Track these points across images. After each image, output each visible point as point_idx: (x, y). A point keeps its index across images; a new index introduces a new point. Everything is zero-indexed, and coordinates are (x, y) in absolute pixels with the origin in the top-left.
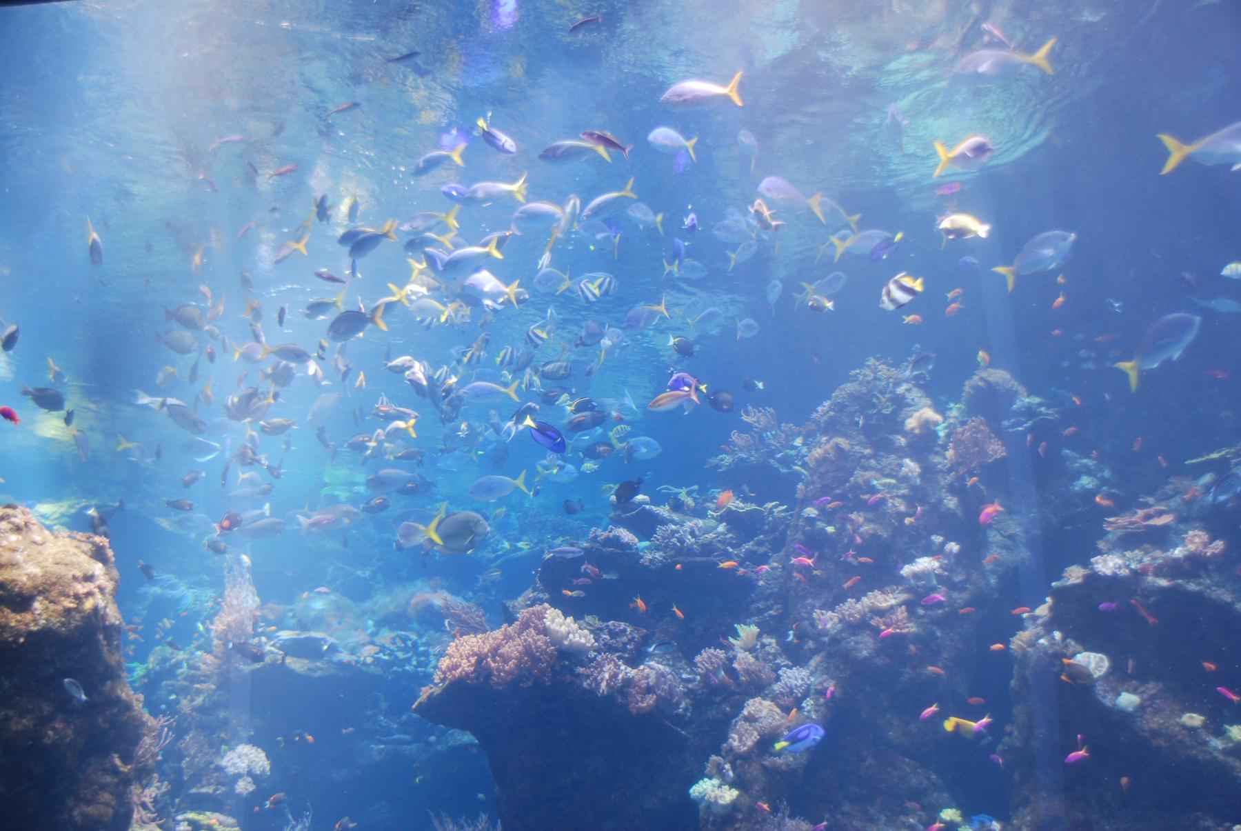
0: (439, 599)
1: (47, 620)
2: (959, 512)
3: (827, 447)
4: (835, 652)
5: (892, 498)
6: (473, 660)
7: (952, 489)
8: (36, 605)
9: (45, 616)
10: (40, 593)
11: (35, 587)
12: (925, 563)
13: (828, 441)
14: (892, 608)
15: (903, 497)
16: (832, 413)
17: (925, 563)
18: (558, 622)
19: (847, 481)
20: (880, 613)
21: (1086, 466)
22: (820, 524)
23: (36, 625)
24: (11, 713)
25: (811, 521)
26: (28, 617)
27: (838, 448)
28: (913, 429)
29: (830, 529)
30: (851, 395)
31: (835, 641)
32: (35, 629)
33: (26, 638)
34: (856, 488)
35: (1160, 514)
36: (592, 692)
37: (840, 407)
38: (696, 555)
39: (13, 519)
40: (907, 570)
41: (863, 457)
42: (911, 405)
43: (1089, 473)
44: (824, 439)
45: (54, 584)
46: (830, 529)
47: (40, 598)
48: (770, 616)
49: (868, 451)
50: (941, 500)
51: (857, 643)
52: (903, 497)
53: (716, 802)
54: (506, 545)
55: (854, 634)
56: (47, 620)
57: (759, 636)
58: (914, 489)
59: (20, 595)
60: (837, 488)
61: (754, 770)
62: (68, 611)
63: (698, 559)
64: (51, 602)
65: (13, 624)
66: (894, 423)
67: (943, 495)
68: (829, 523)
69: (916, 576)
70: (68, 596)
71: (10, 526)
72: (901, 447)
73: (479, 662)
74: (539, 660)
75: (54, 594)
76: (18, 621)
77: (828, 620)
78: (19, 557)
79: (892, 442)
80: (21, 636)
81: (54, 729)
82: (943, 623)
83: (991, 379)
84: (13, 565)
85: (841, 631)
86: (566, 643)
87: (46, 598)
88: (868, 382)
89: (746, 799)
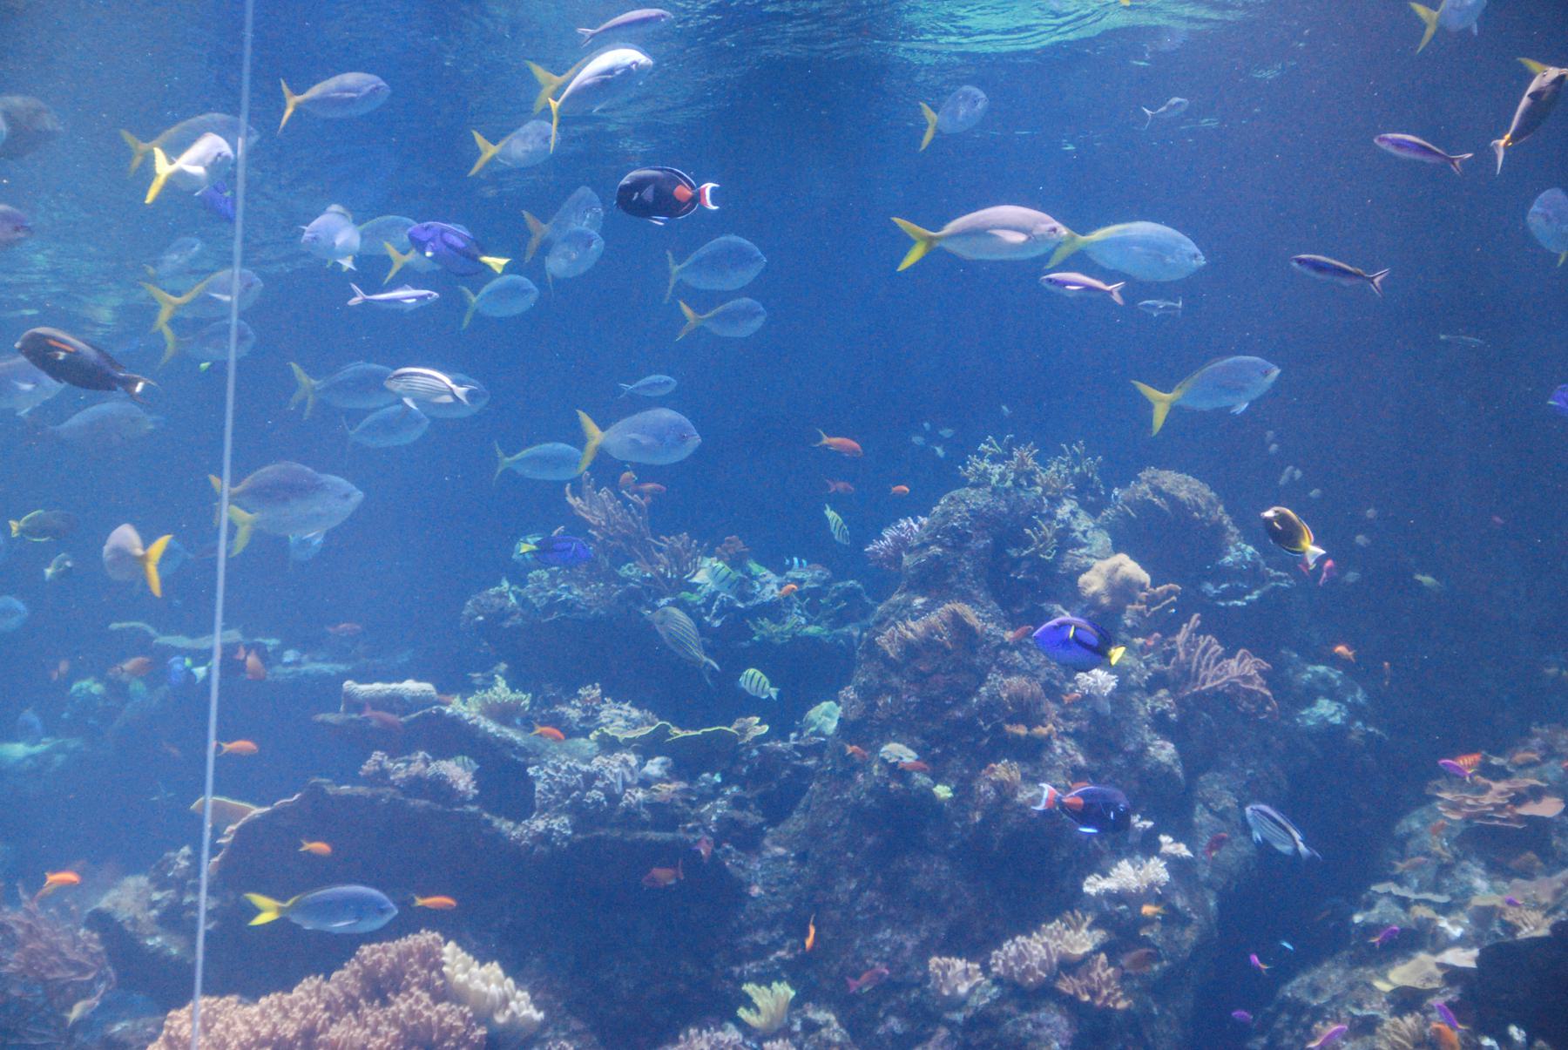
2: (1178, 770)
3: (933, 618)
5: (1061, 736)
7: (1160, 723)
12: (1126, 875)
13: (927, 609)
14: (1086, 959)
15: (1076, 735)
16: (936, 550)
17: (1126, 875)
18: (485, 980)
19: (975, 692)
20: (1070, 966)
21: (1325, 679)
22: (921, 780)
25: (896, 771)
27: (957, 621)
28: (1096, 596)
29: (943, 791)
30: (976, 514)
31: (983, 1020)
34: (992, 707)
35: (1536, 794)
37: (958, 539)
38: (644, 826)
40: (1093, 885)
41: (1004, 645)
43: (1332, 695)
44: (918, 602)
48: (779, 959)
50: (1143, 748)
51: (1038, 1025)
55: (1025, 1007)
57: (796, 1004)
58: (1096, 717)
60: (955, 705)
63: (652, 835)
66: (1063, 585)
67: (1147, 737)
68: (937, 778)
69: (1110, 896)
82: (1160, 989)
83: (1183, 495)
85: (1000, 1001)
88: (1007, 491)
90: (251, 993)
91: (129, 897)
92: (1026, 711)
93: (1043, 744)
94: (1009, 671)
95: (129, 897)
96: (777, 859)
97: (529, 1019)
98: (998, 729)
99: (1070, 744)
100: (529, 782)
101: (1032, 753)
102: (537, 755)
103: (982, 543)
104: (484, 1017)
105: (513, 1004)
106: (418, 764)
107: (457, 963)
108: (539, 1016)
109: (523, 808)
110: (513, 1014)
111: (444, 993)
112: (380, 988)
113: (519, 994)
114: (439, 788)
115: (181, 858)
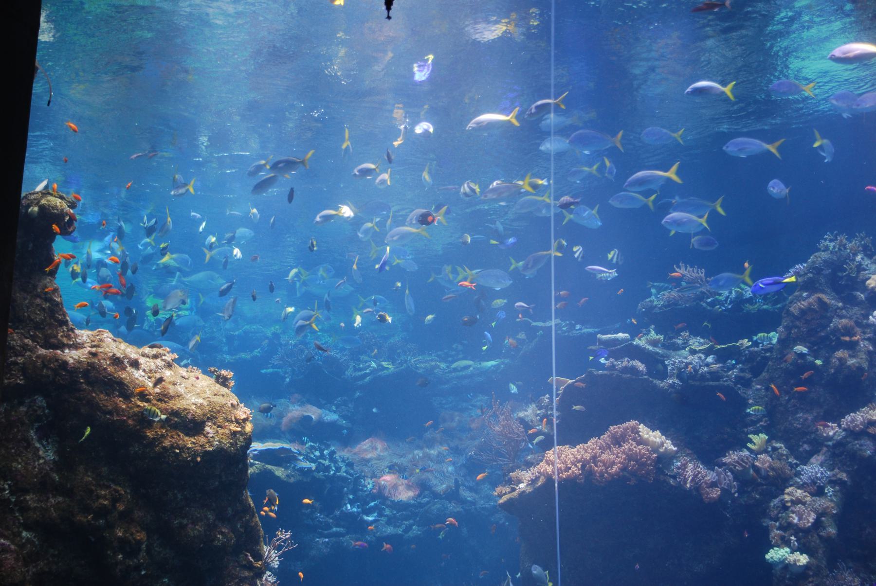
0: (314, 413)
1: (219, 441)
3: (811, 300)
4: (839, 453)
6: (579, 465)
8: (207, 429)
9: (217, 439)
11: (204, 415)
13: (808, 297)
15: (869, 339)
18: (655, 437)
19: (828, 326)
24: (185, 522)
25: (802, 355)
26: (202, 440)
27: (820, 300)
29: (818, 362)
30: (825, 261)
31: (839, 444)
33: (202, 458)
34: (836, 331)
36: (680, 487)
37: (817, 271)
38: (708, 380)
39: (164, 357)
41: (838, 308)
42: (866, 270)
44: (805, 294)
45: (219, 412)
46: (818, 362)
49: (840, 304)
51: (861, 445)
52: (869, 339)
53: (795, 564)
54: (373, 364)
55: (856, 439)
57: (768, 441)
59: (193, 421)
61: (814, 539)
62: (234, 433)
63: (711, 383)
65: (190, 446)
71: (163, 363)
72: (862, 301)
73: (583, 466)
74: (644, 464)
75: (220, 419)
76: (194, 443)
77: (832, 431)
78: (181, 389)
79: (855, 297)
80: (198, 455)
81: (222, 533)
84: (179, 396)
85: (845, 438)
86: (661, 450)
87: (215, 424)
89: (814, 561)
90: (573, 444)
92: (849, 332)
93: (856, 343)
94: (841, 317)
96: (757, 390)
97: (671, 450)
98: (838, 339)
99: (866, 343)
101: (852, 346)
102: (668, 357)
103: (827, 272)
104: (655, 449)
106: (625, 362)
107: (645, 432)
108: (675, 449)
109: (663, 375)
111: (641, 442)
112: (618, 441)
114: (633, 370)
115: (546, 399)
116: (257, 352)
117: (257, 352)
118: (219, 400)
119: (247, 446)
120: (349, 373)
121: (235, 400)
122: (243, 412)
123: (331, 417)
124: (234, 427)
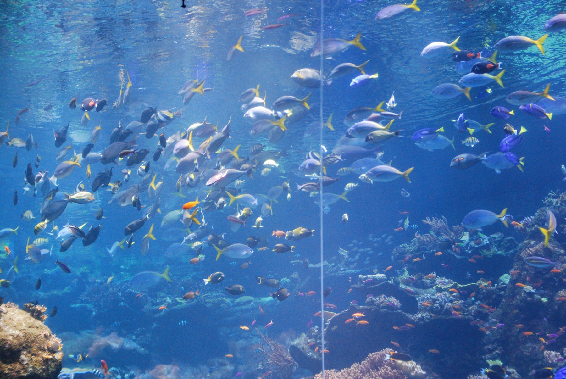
0: (114, 342)
1: (33, 367)
3: (537, 247)
8: (23, 357)
9: (31, 365)
10: (24, 348)
11: (20, 345)
13: (536, 244)
22: (537, 297)
23: (26, 371)
25: (530, 294)
26: (18, 366)
29: (544, 300)
32: (25, 374)
41: (561, 254)
44: (532, 242)
45: (33, 342)
46: (544, 300)
47: (25, 352)
48: (496, 353)
49: (562, 251)
54: (169, 300)
56: (33, 367)
59: (10, 350)
62: (46, 361)
64: (33, 355)
65: (7, 372)
70: (44, 350)
75: (34, 349)
76: (9, 369)
86: (413, 374)
87: (29, 352)
88: (559, 207)
91: (301, 341)
95: (301, 341)
97: (421, 373)
100: (416, 302)
102: (418, 294)
105: (416, 369)
108: (424, 373)
109: (414, 310)
110: (416, 372)
113: (418, 366)
114: (390, 307)
115: (315, 329)
116: (67, 290)
117: (67, 290)
118: (34, 331)
119: (58, 371)
120: (147, 307)
121: (47, 331)
122: (55, 341)
123: (130, 345)
124: (46, 355)
